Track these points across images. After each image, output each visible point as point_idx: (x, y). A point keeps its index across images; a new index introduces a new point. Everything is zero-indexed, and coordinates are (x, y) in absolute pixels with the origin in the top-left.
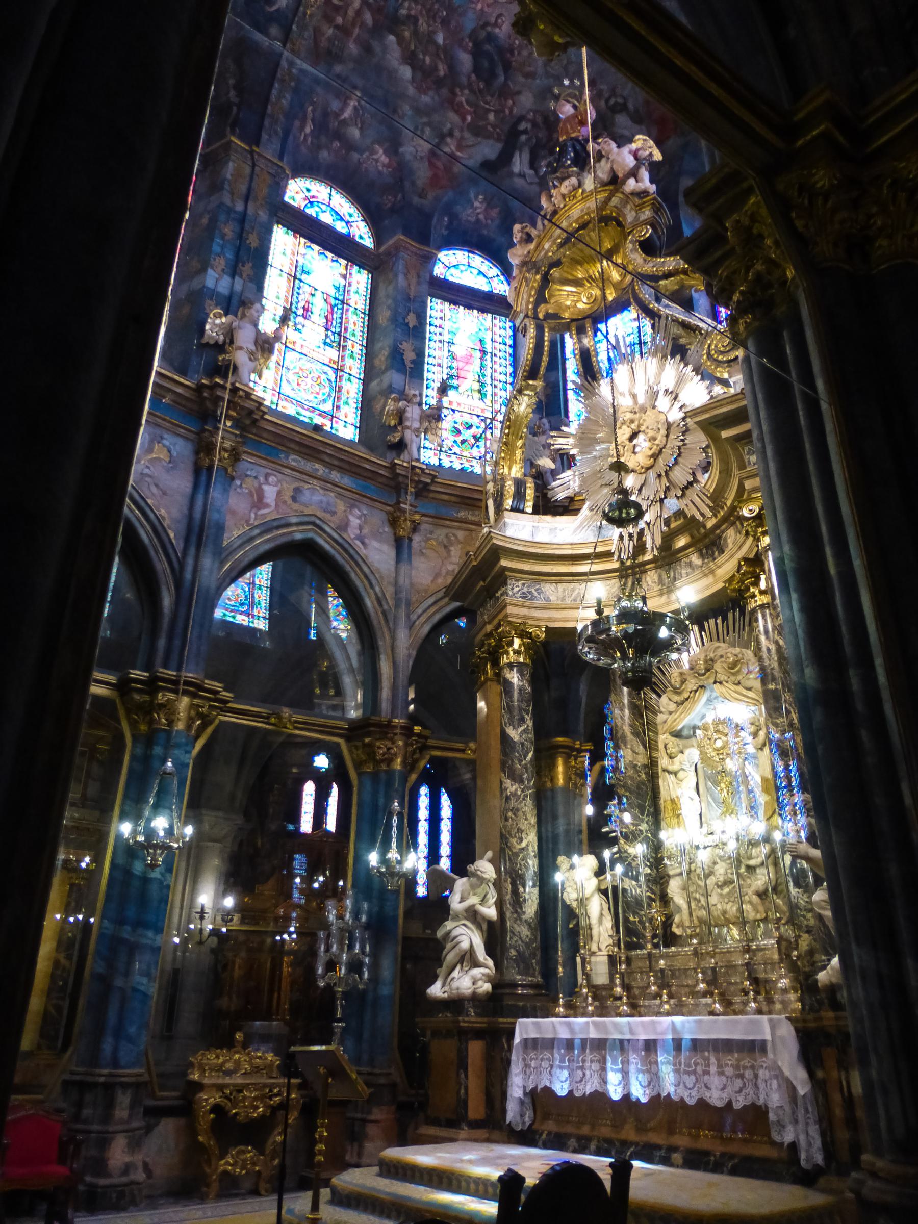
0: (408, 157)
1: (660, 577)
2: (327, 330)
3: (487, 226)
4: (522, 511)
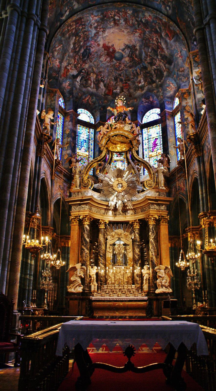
0: (62, 66)
1: (113, 213)
3: (66, 89)
4: (90, 189)
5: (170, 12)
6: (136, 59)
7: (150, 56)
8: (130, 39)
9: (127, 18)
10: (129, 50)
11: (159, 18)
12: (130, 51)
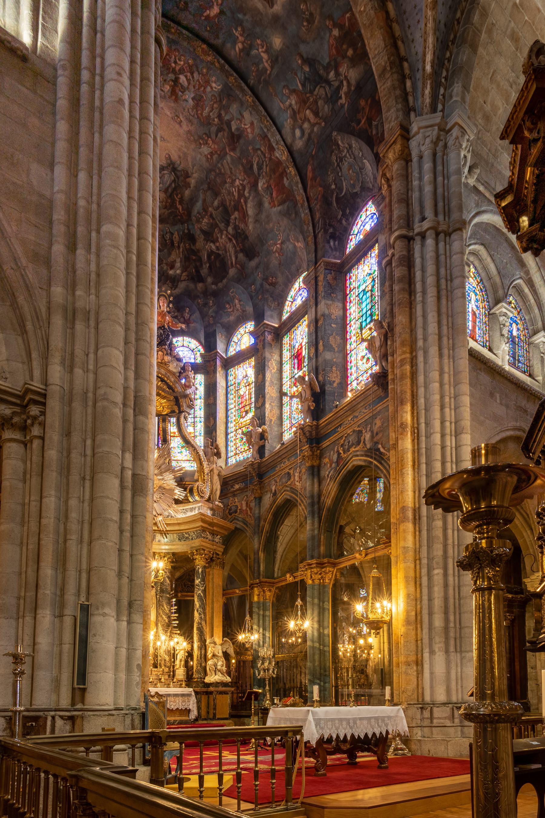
5: (299, 144)
6: (180, 207)
7: (211, 215)
8: (186, 150)
9: (202, 97)
10: (173, 178)
11: (269, 140)
12: (174, 181)
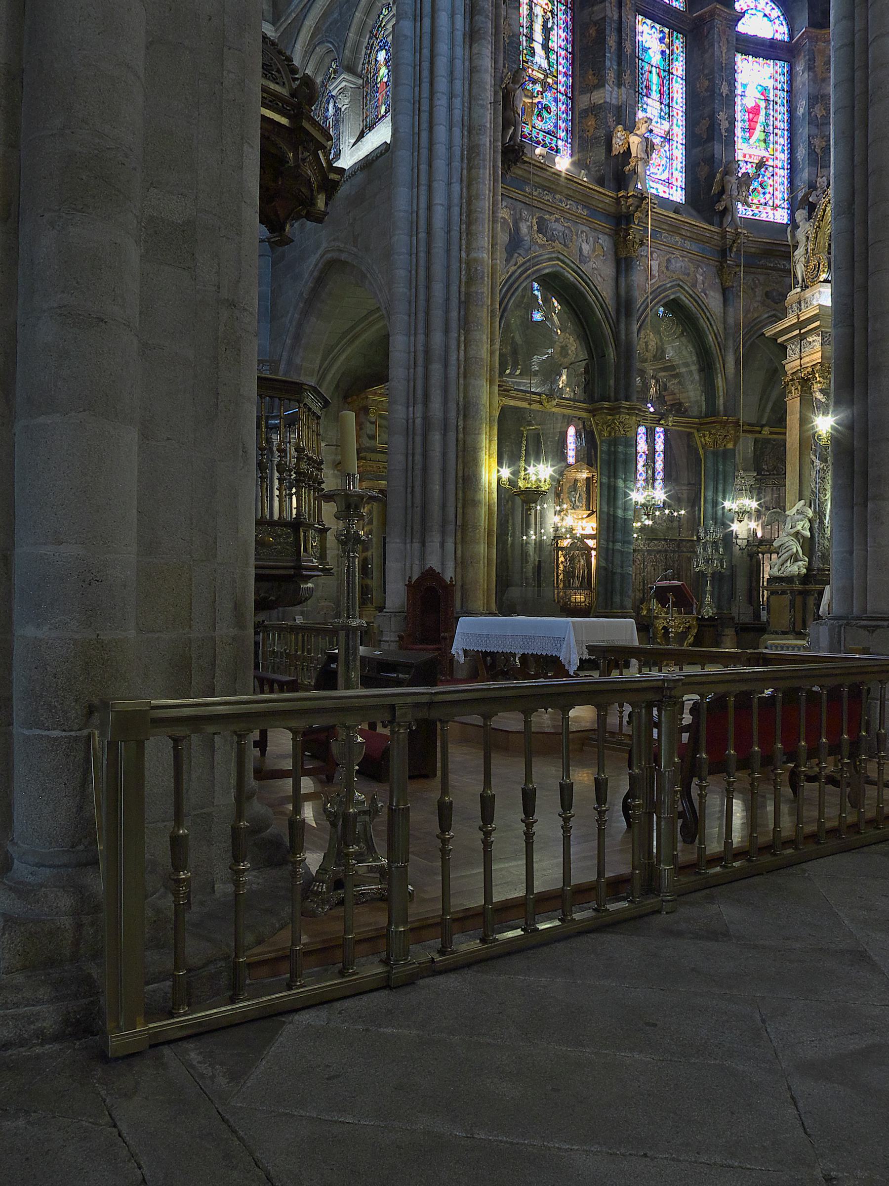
2: (661, 103)
